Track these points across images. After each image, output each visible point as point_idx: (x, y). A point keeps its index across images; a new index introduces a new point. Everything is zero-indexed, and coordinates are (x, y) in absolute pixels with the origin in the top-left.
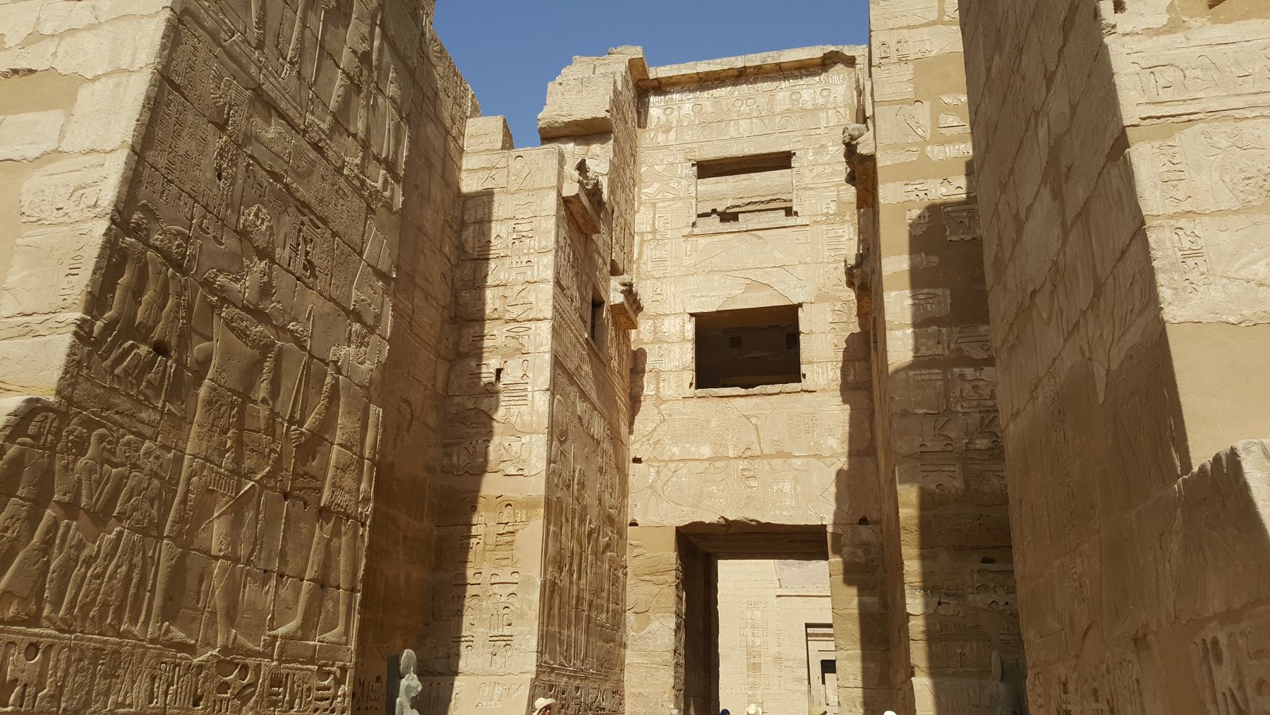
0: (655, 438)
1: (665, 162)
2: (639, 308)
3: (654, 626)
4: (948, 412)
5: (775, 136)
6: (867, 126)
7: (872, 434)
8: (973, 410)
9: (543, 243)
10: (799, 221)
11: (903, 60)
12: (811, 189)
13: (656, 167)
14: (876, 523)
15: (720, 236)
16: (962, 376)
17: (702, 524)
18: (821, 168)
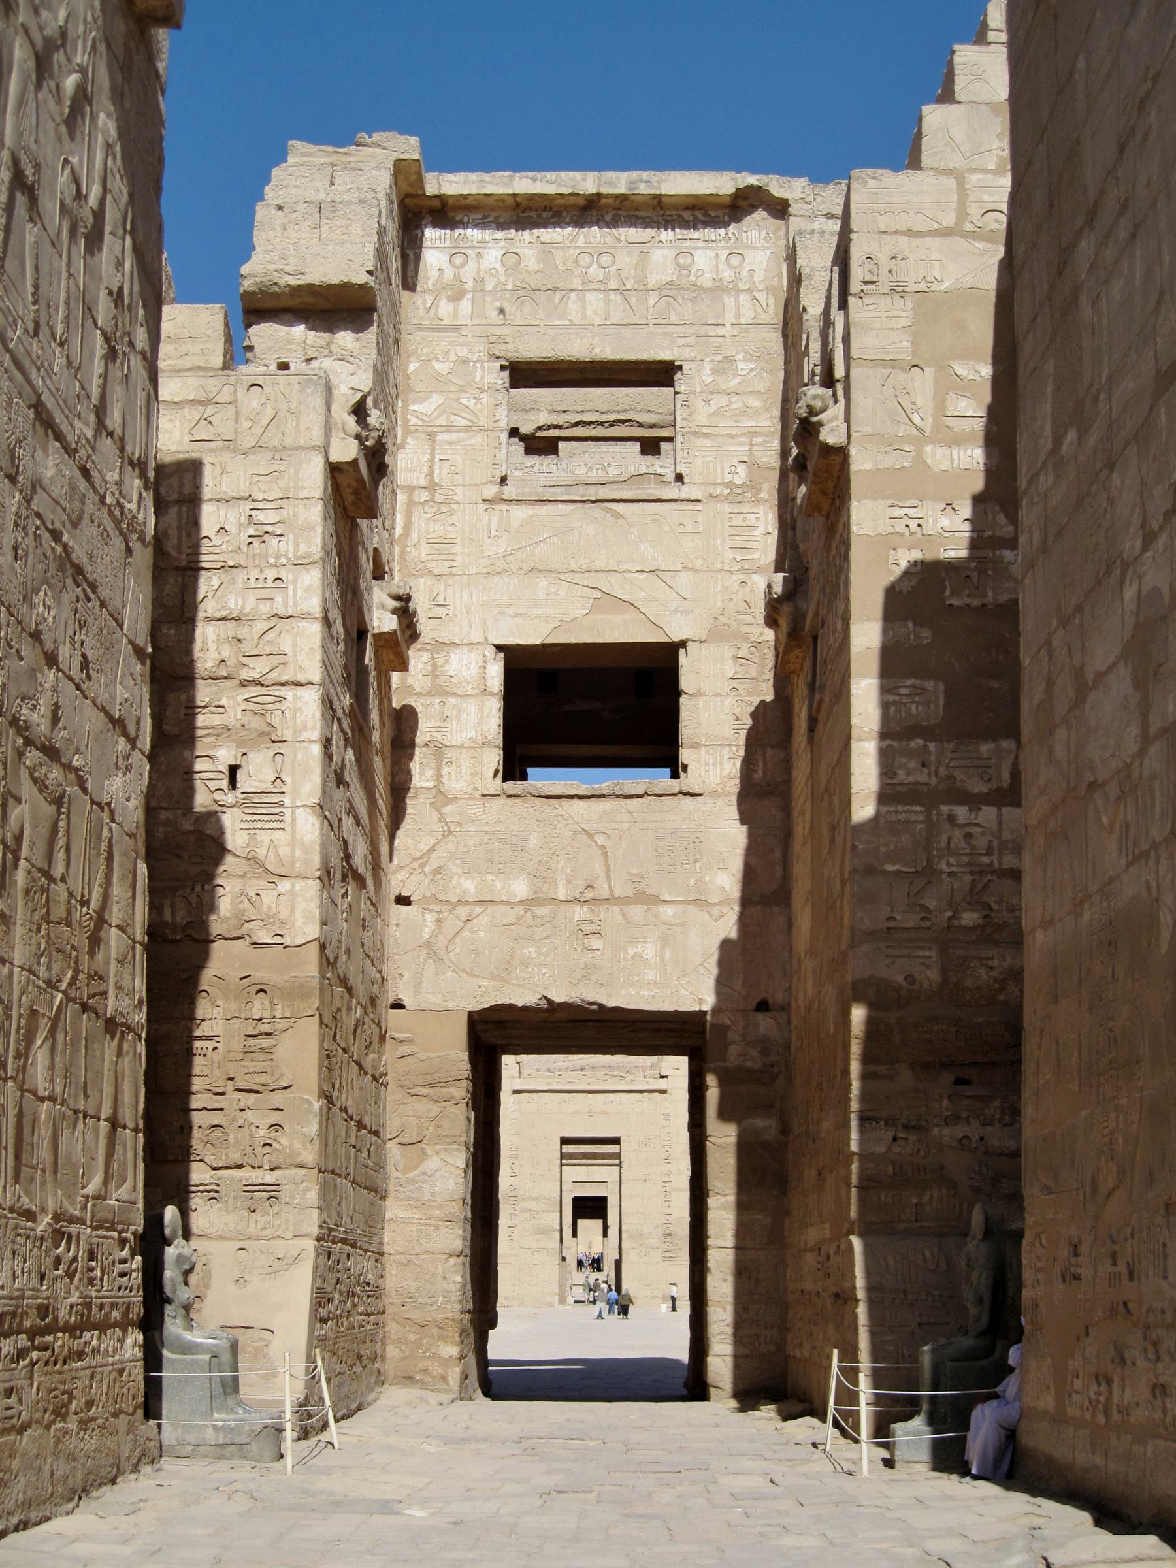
0: (434, 863)
1: (453, 358)
2: (414, 636)
4: (929, 873)
5: (646, 330)
6: (834, 395)
8: (962, 869)
10: (686, 492)
11: (898, 290)
12: (706, 435)
13: (434, 363)
15: (550, 507)
16: (951, 818)
17: (511, 1007)
18: (724, 400)
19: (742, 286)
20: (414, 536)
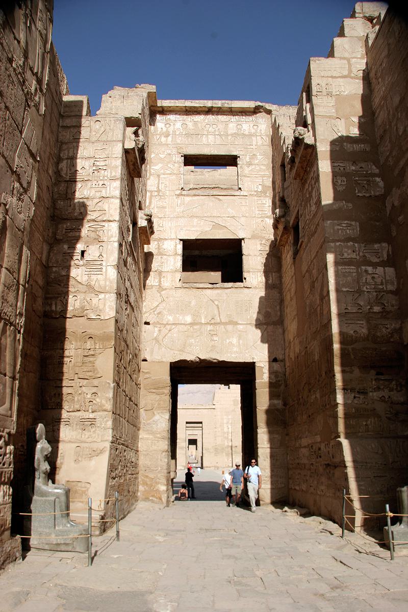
0: (158, 310)
2: (152, 232)
3: (157, 417)
4: (360, 292)
6: (308, 129)
7: (281, 313)
8: (372, 290)
9: (114, 174)
11: (329, 94)
12: (248, 177)
13: (161, 156)
14: (282, 361)
15: (198, 197)
16: (366, 271)
17: (185, 361)
19: (258, 134)
20: (153, 206)
